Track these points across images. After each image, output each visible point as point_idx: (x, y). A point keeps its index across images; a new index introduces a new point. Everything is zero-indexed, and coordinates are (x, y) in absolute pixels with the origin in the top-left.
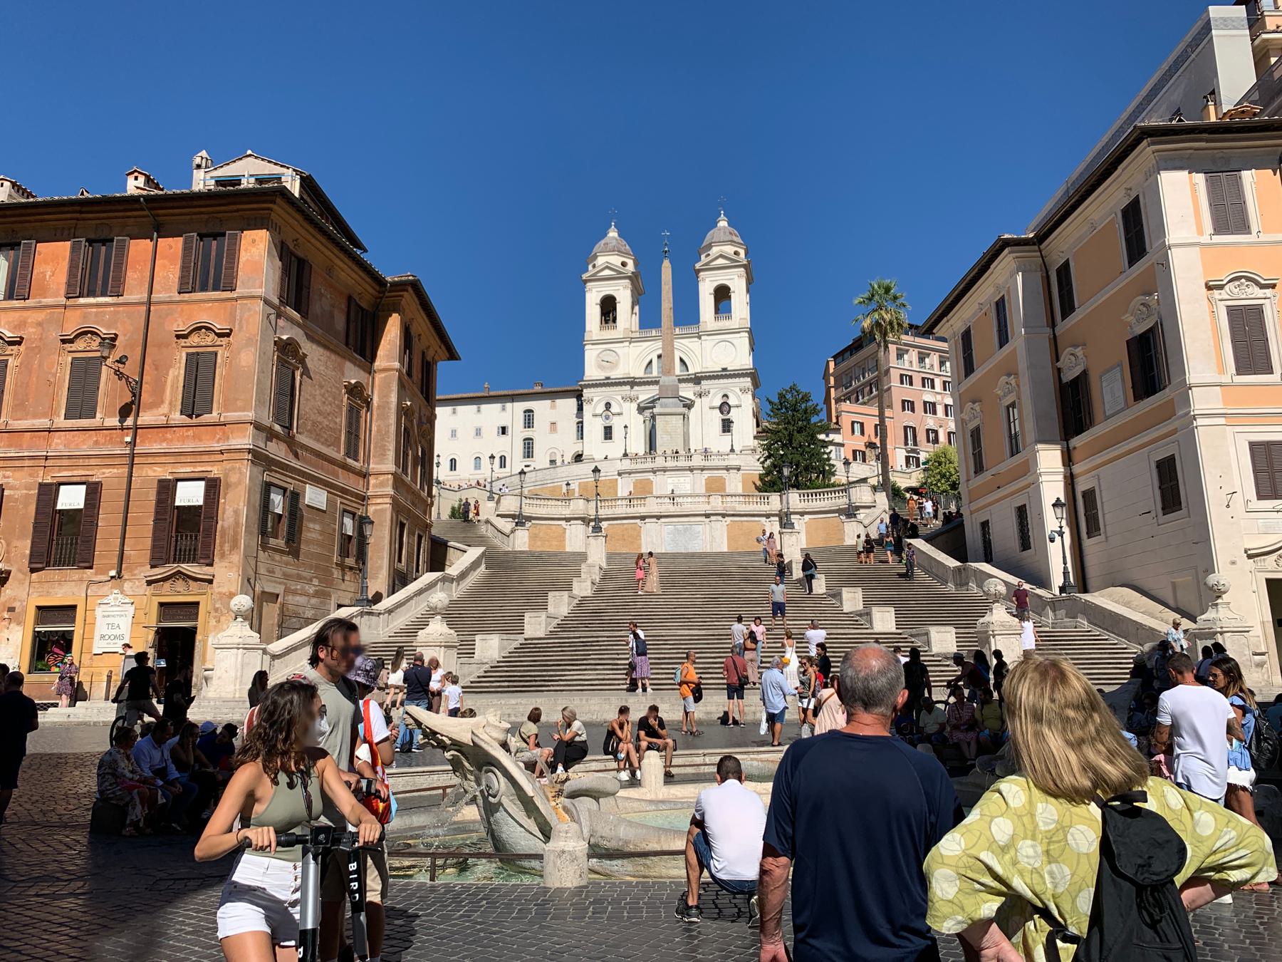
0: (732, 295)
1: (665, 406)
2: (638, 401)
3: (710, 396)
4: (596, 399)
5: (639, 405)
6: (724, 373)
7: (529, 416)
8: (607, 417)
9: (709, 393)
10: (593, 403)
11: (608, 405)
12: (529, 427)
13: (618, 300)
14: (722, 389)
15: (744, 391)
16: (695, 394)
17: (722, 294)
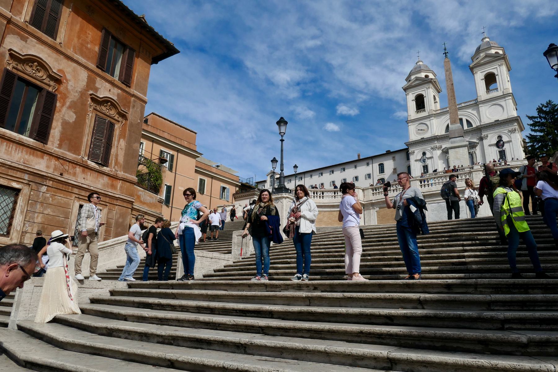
0: (497, 77)
1: (454, 142)
2: (442, 149)
3: (488, 138)
4: (416, 152)
5: (442, 150)
6: (496, 123)
7: (381, 167)
8: (424, 161)
9: (487, 136)
10: (415, 154)
11: (424, 154)
12: (382, 173)
13: (424, 95)
14: (496, 133)
15: (513, 131)
16: (478, 139)
17: (490, 79)
